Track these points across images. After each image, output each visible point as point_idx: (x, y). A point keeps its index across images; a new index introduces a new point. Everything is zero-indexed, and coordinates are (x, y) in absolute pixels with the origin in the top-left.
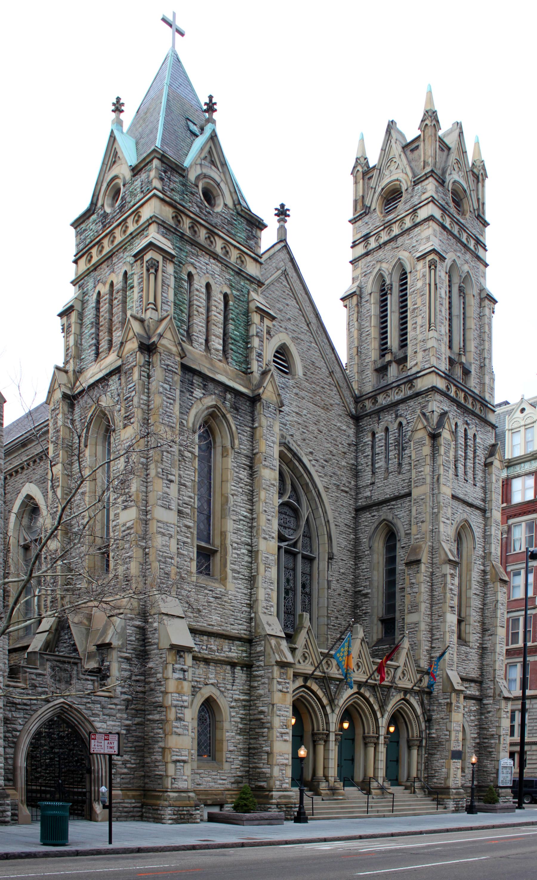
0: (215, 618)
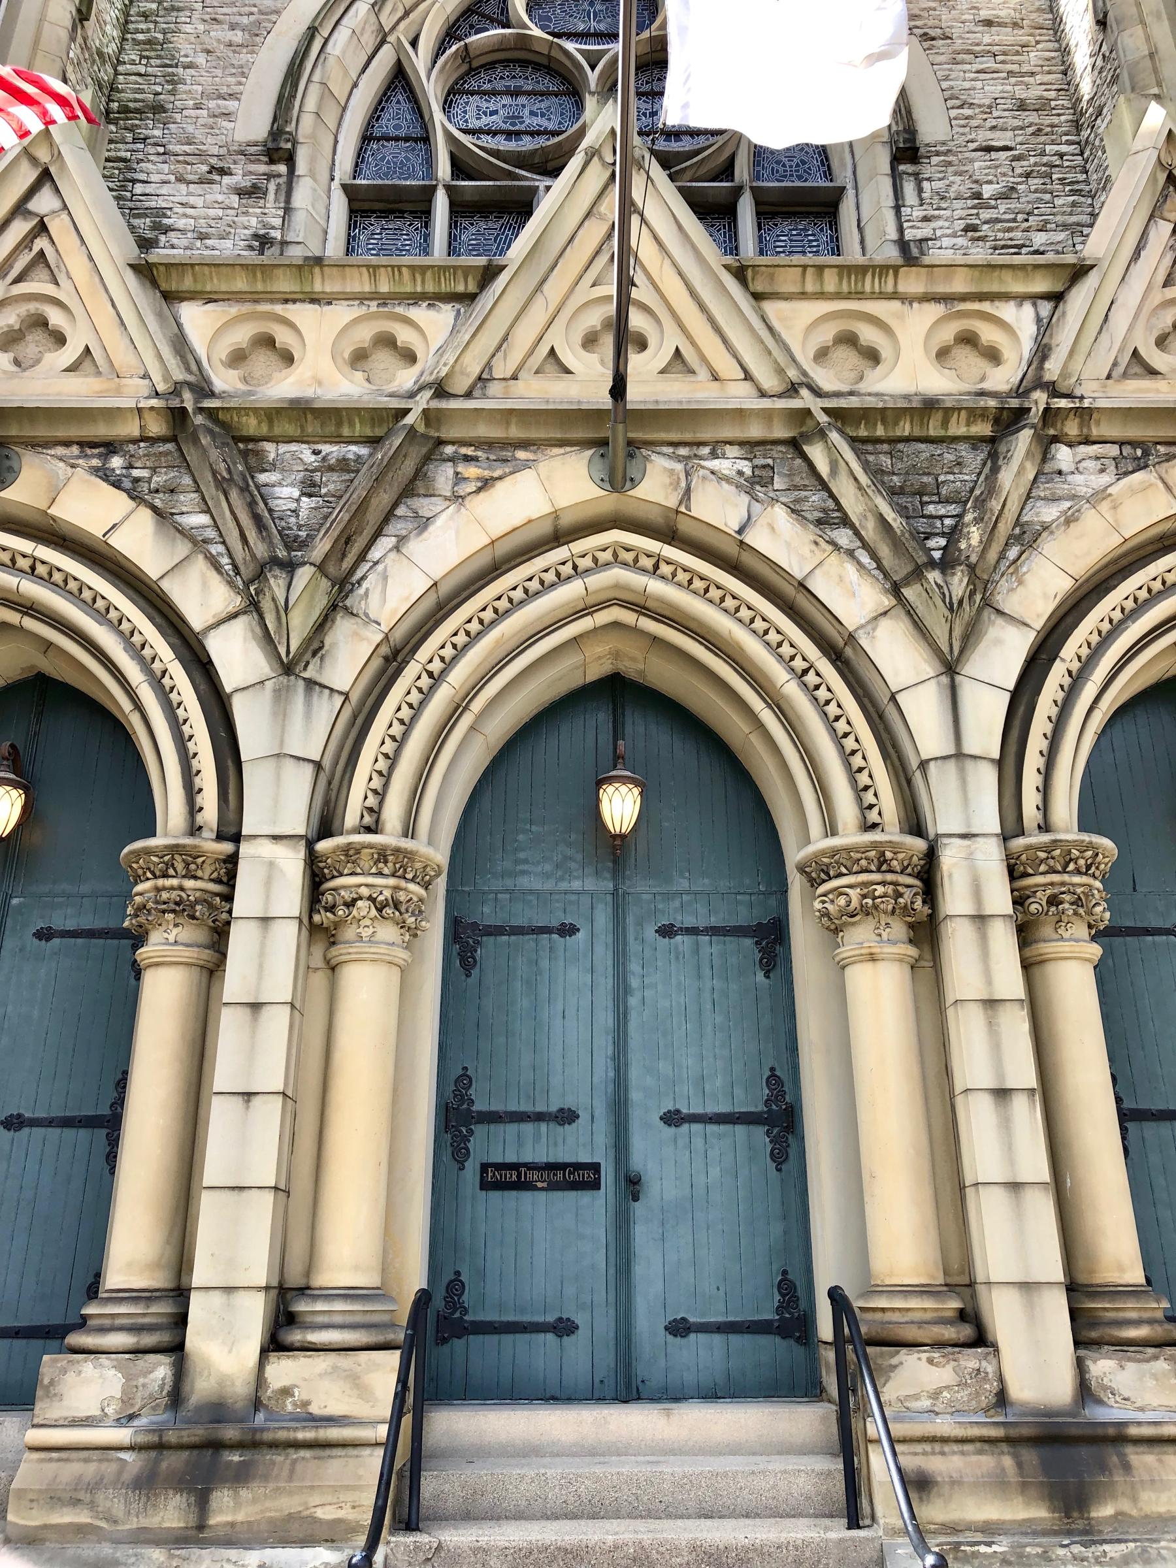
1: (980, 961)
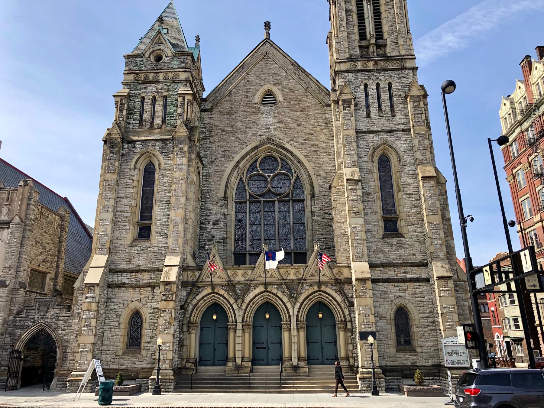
0: (142, 262)
1: (294, 333)
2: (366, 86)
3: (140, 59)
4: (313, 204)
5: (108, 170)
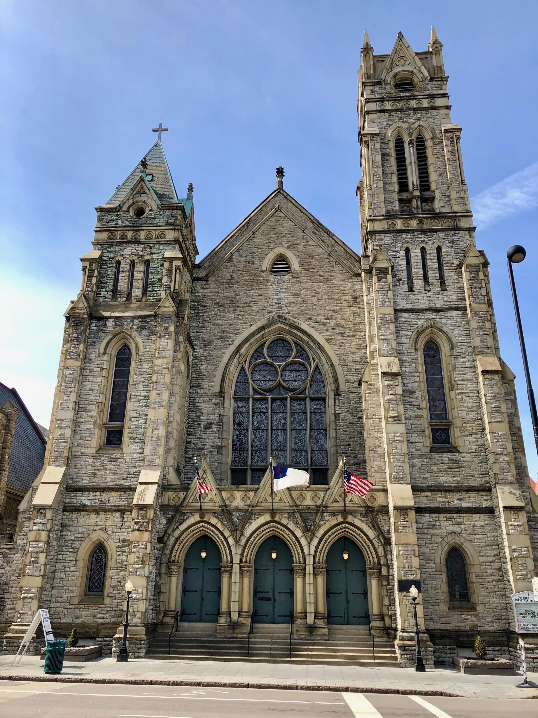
0: (110, 477)
1: (310, 579)
2: (407, 251)
3: (116, 213)
4: (337, 404)
5: (70, 355)
